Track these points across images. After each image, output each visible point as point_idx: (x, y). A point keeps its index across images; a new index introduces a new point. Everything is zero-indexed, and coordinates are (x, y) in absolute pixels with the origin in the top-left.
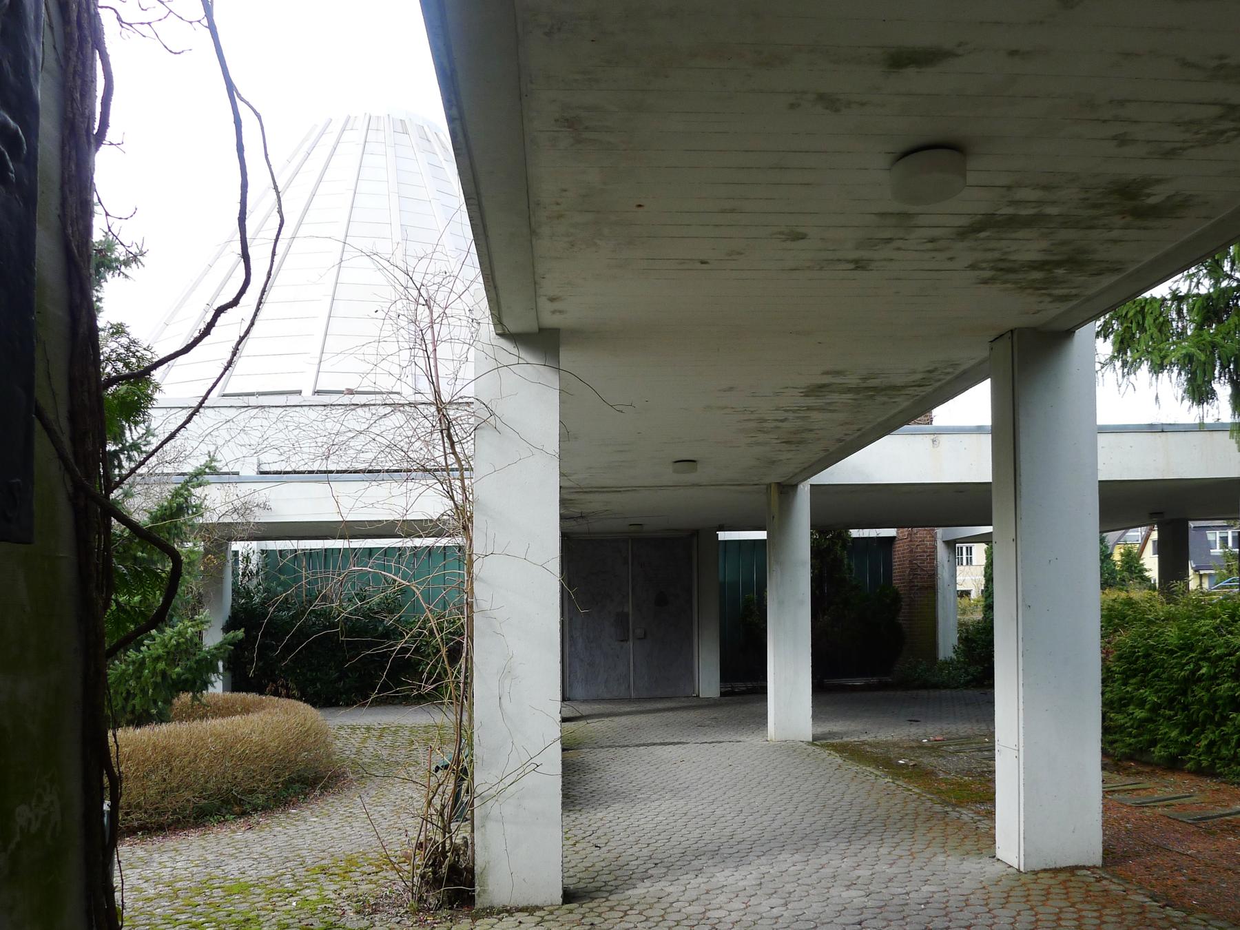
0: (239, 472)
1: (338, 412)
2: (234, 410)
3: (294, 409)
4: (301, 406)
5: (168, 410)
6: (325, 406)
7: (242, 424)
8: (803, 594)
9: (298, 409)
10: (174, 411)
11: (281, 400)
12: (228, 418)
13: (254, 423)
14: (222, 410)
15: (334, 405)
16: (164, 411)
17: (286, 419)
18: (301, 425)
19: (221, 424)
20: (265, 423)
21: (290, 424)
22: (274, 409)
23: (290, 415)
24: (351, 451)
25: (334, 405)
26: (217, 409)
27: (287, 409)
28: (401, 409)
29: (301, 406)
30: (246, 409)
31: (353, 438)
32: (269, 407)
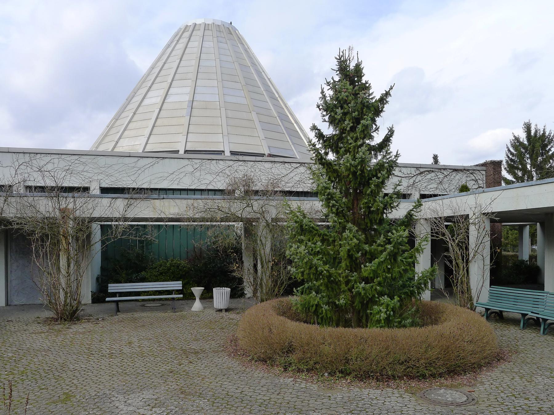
0: (525, 124)
1: (278, 165)
2: (232, 161)
3: (258, 163)
4: (261, 161)
5: (202, 160)
6: (271, 162)
7: (236, 168)
8: (447, 379)
9: (260, 163)
10: (204, 161)
11: (253, 158)
12: (229, 165)
13: (241, 168)
14: (227, 161)
15: (276, 162)
16: (200, 160)
17: (256, 167)
18: (261, 170)
19: (226, 168)
20: (246, 168)
21: (257, 169)
22: (250, 162)
23: (257, 165)
24: (283, 182)
25: (276, 162)
26: (224, 161)
27: (255, 162)
28: (304, 165)
29: (261, 161)
30: (237, 161)
31: (284, 176)
32: (248, 161)
